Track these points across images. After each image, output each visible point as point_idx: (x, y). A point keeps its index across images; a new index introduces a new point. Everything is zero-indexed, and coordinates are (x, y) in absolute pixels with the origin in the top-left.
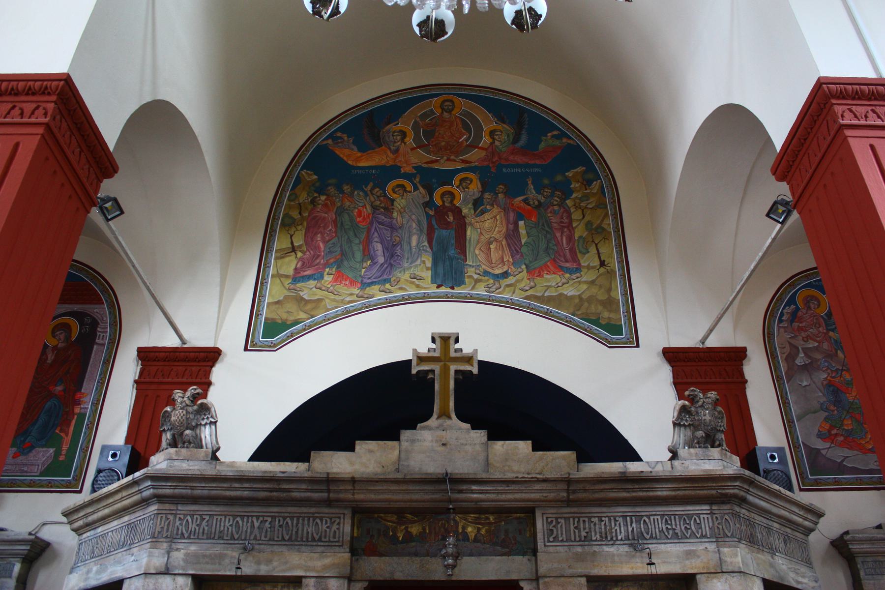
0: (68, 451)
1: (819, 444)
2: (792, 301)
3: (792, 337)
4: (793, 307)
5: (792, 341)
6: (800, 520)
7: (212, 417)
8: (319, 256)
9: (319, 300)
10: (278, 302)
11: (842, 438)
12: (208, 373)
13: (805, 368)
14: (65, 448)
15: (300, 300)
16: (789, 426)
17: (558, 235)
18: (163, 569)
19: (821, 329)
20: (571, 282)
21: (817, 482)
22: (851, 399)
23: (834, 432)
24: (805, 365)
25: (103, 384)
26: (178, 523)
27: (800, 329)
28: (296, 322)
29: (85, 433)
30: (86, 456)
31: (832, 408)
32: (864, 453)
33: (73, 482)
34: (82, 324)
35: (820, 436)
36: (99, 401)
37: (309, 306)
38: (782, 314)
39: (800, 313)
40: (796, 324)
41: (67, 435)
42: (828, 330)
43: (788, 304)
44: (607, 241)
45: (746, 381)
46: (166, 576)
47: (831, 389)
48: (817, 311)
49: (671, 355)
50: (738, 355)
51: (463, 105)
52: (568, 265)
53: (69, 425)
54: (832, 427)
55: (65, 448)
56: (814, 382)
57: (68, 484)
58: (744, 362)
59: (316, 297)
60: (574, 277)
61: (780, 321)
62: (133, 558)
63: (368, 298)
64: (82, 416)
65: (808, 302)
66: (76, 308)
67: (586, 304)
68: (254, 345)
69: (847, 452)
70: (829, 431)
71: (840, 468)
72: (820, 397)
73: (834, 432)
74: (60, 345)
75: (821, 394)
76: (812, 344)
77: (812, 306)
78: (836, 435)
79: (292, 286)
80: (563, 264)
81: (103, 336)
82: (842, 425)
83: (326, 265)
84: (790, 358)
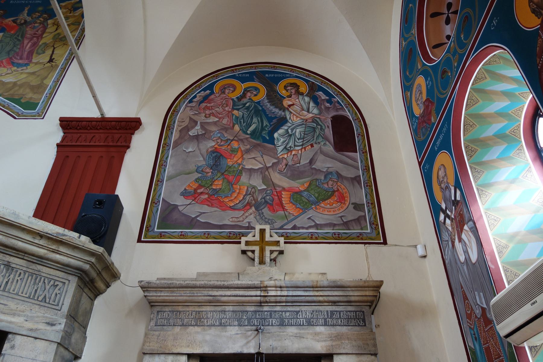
1: (179, 201)
2: (211, 87)
3: (196, 114)
4: (208, 92)
5: (192, 117)
6: (42, 252)
11: (206, 196)
13: (197, 138)
16: (157, 185)
17: (26, 42)
19: (226, 109)
20: (14, 73)
21: (161, 235)
22: (230, 164)
23: (199, 191)
24: (198, 135)
27: (207, 108)
31: (208, 170)
32: (223, 210)
35: (185, 194)
38: (195, 97)
39: (212, 96)
40: (204, 105)
42: (233, 109)
43: (205, 90)
44: (65, 46)
45: (128, 147)
47: (214, 155)
48: (230, 95)
49: (66, 124)
50: (132, 125)
52: (20, 61)
54: (200, 186)
56: (200, 149)
58: (136, 132)
60: (19, 69)
61: (191, 101)
65: (225, 88)
67: (17, 88)
69: (205, 208)
70: (195, 190)
71: (193, 223)
72: (201, 161)
73: (199, 191)
75: (202, 159)
76: (213, 119)
77: (227, 91)
78: (202, 193)
80: (16, 61)
82: (211, 185)
84: (185, 131)
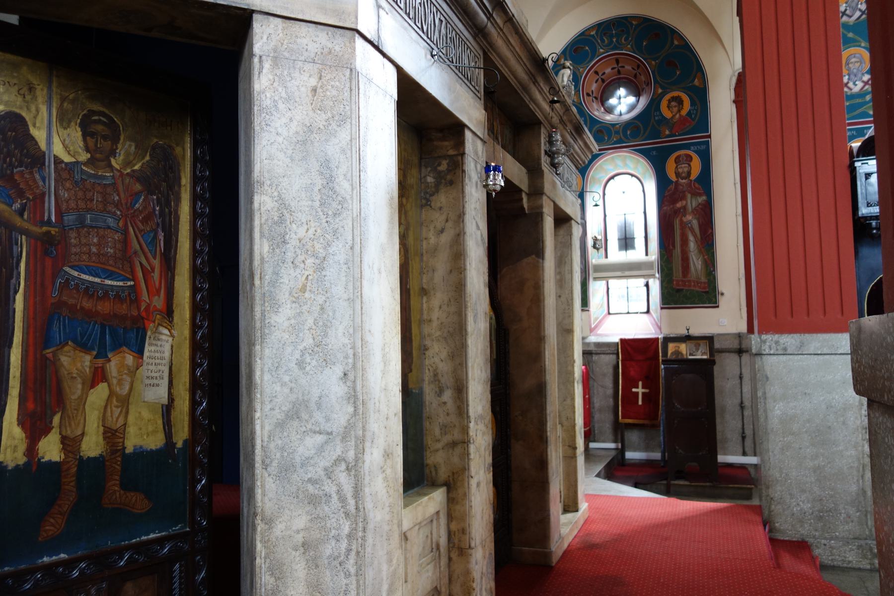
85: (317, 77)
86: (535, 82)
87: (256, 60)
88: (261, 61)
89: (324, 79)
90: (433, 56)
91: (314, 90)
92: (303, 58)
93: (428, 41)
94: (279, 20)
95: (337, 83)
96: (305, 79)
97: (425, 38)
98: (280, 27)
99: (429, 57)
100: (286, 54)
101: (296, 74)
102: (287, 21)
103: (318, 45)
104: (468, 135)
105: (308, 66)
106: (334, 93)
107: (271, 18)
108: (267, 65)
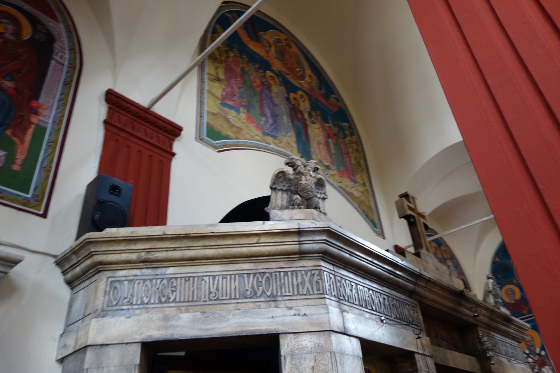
0: (25, 160)
7: (324, 193)
8: (235, 96)
9: (240, 129)
10: (213, 114)
12: (171, 146)
14: (20, 157)
15: (228, 121)
18: (342, 330)
25: (65, 105)
26: (338, 284)
28: (227, 137)
29: (46, 150)
30: (47, 177)
33: (33, 203)
34: (35, 30)
36: (61, 121)
37: (234, 129)
41: (22, 142)
46: (345, 336)
51: (294, 50)
53: (24, 132)
55: (20, 157)
57: (26, 202)
59: (238, 125)
62: (293, 312)
63: (266, 143)
64: (40, 131)
66: (26, 7)
68: (201, 139)
74: (7, 35)
79: (222, 107)
81: (62, 55)
83: (240, 105)
85: (313, 360)
86: (461, 305)
87: (282, 358)
88: (285, 358)
89: (317, 361)
90: (382, 321)
91: (313, 368)
92: (305, 352)
93: (378, 314)
94: (292, 335)
95: (325, 362)
96: (308, 363)
97: (375, 313)
98: (293, 338)
99: (379, 322)
100: (297, 352)
101: (303, 362)
102: (297, 335)
103: (312, 343)
104: (417, 356)
105: (308, 356)
106: (324, 367)
107: (288, 335)
108: (288, 360)
